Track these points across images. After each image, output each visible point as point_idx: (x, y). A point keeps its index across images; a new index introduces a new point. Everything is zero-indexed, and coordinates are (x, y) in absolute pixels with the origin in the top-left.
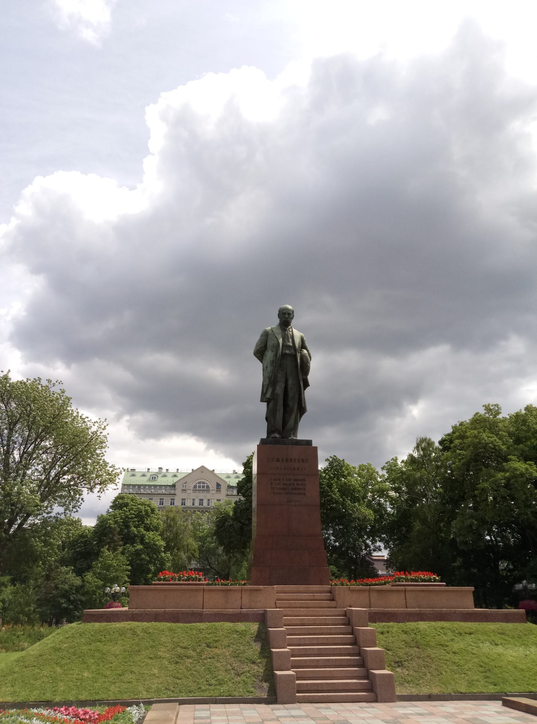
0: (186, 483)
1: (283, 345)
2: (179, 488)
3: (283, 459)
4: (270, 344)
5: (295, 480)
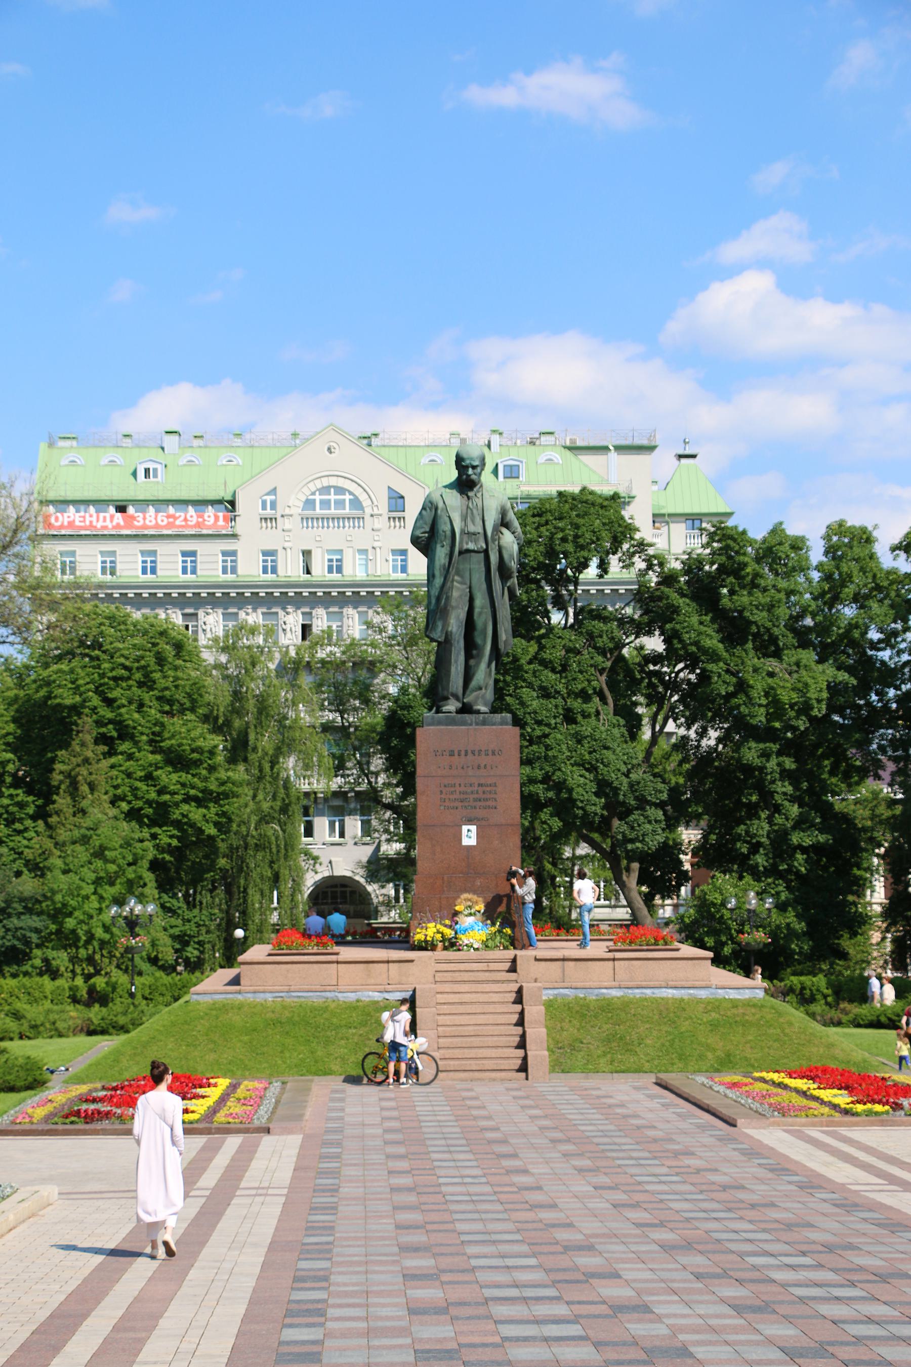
0: (274, 491)
1: (463, 532)
2: (248, 508)
3: (459, 751)
5: (480, 785)
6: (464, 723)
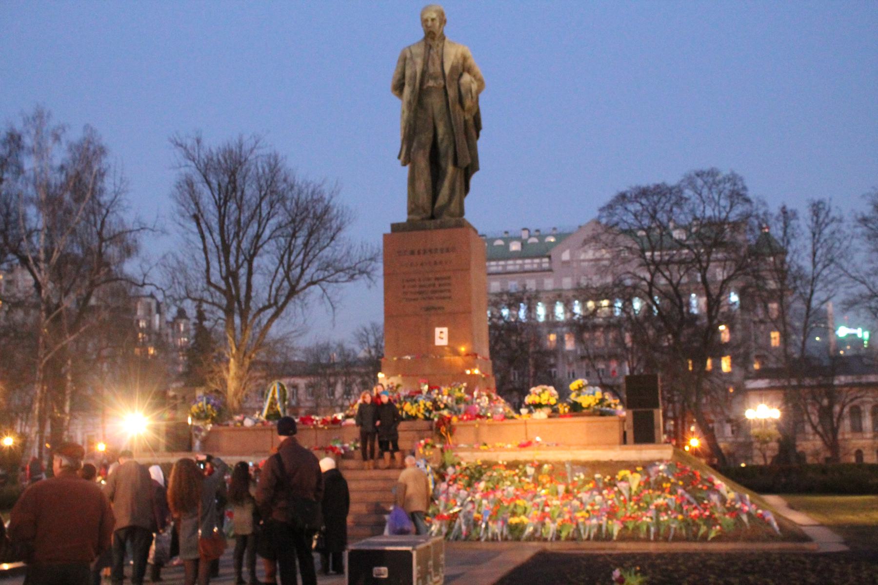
1: (424, 73)
4: (408, 73)
5: (437, 279)
6: (424, 229)
